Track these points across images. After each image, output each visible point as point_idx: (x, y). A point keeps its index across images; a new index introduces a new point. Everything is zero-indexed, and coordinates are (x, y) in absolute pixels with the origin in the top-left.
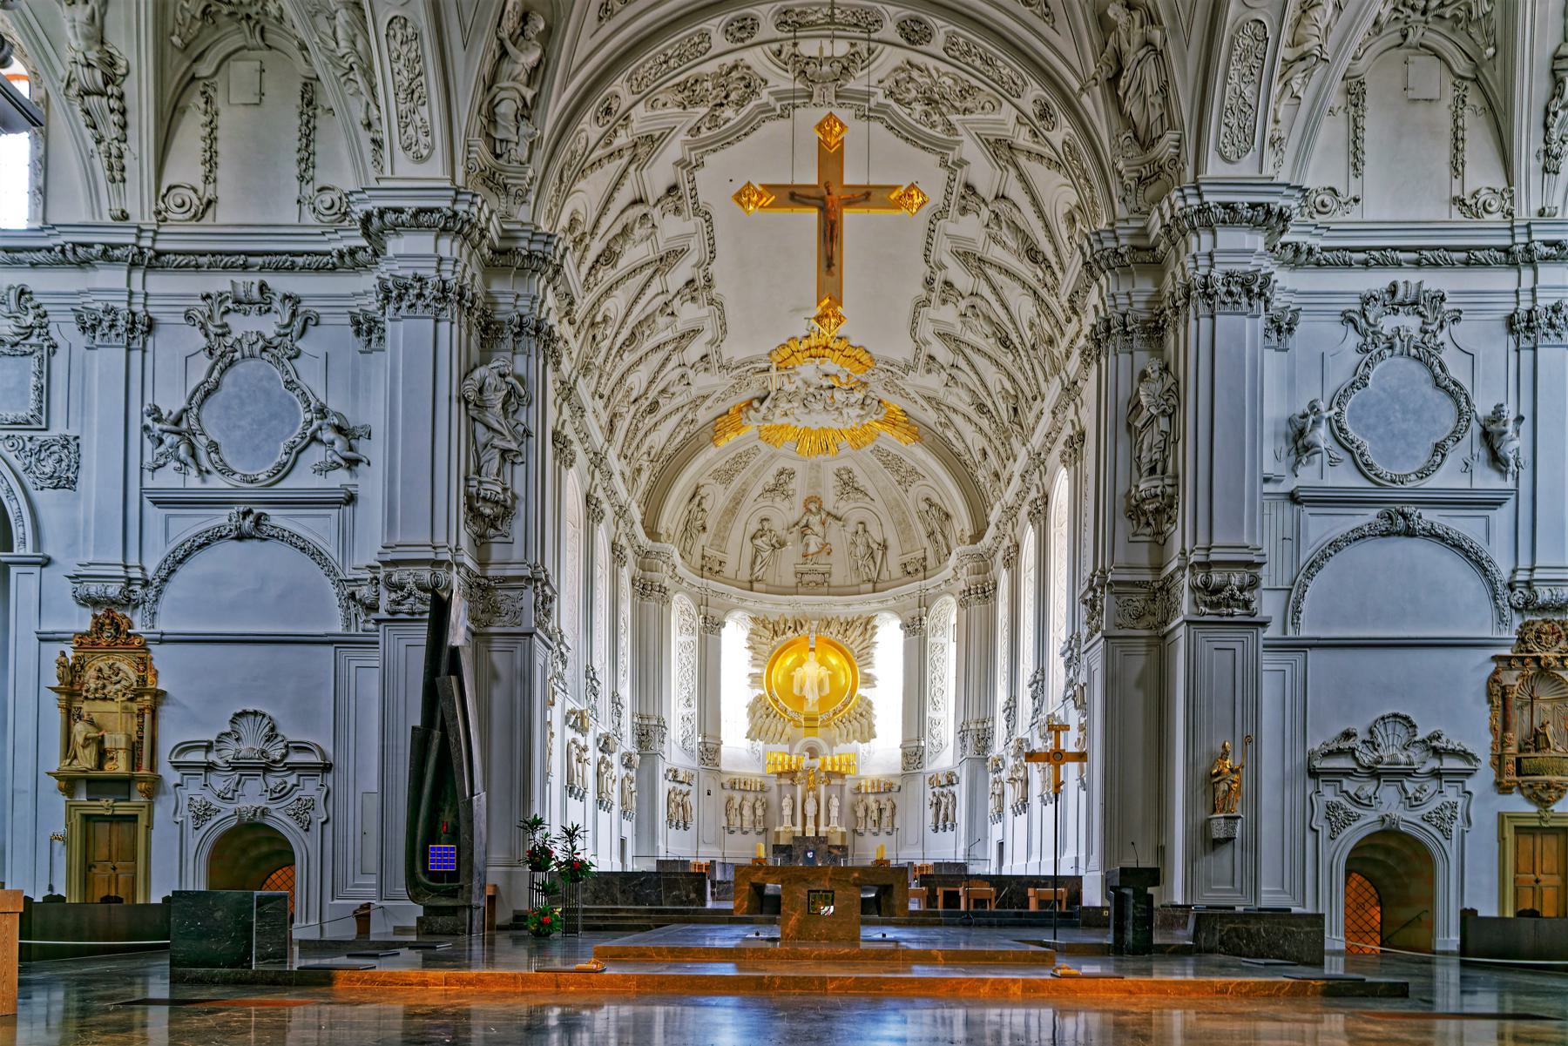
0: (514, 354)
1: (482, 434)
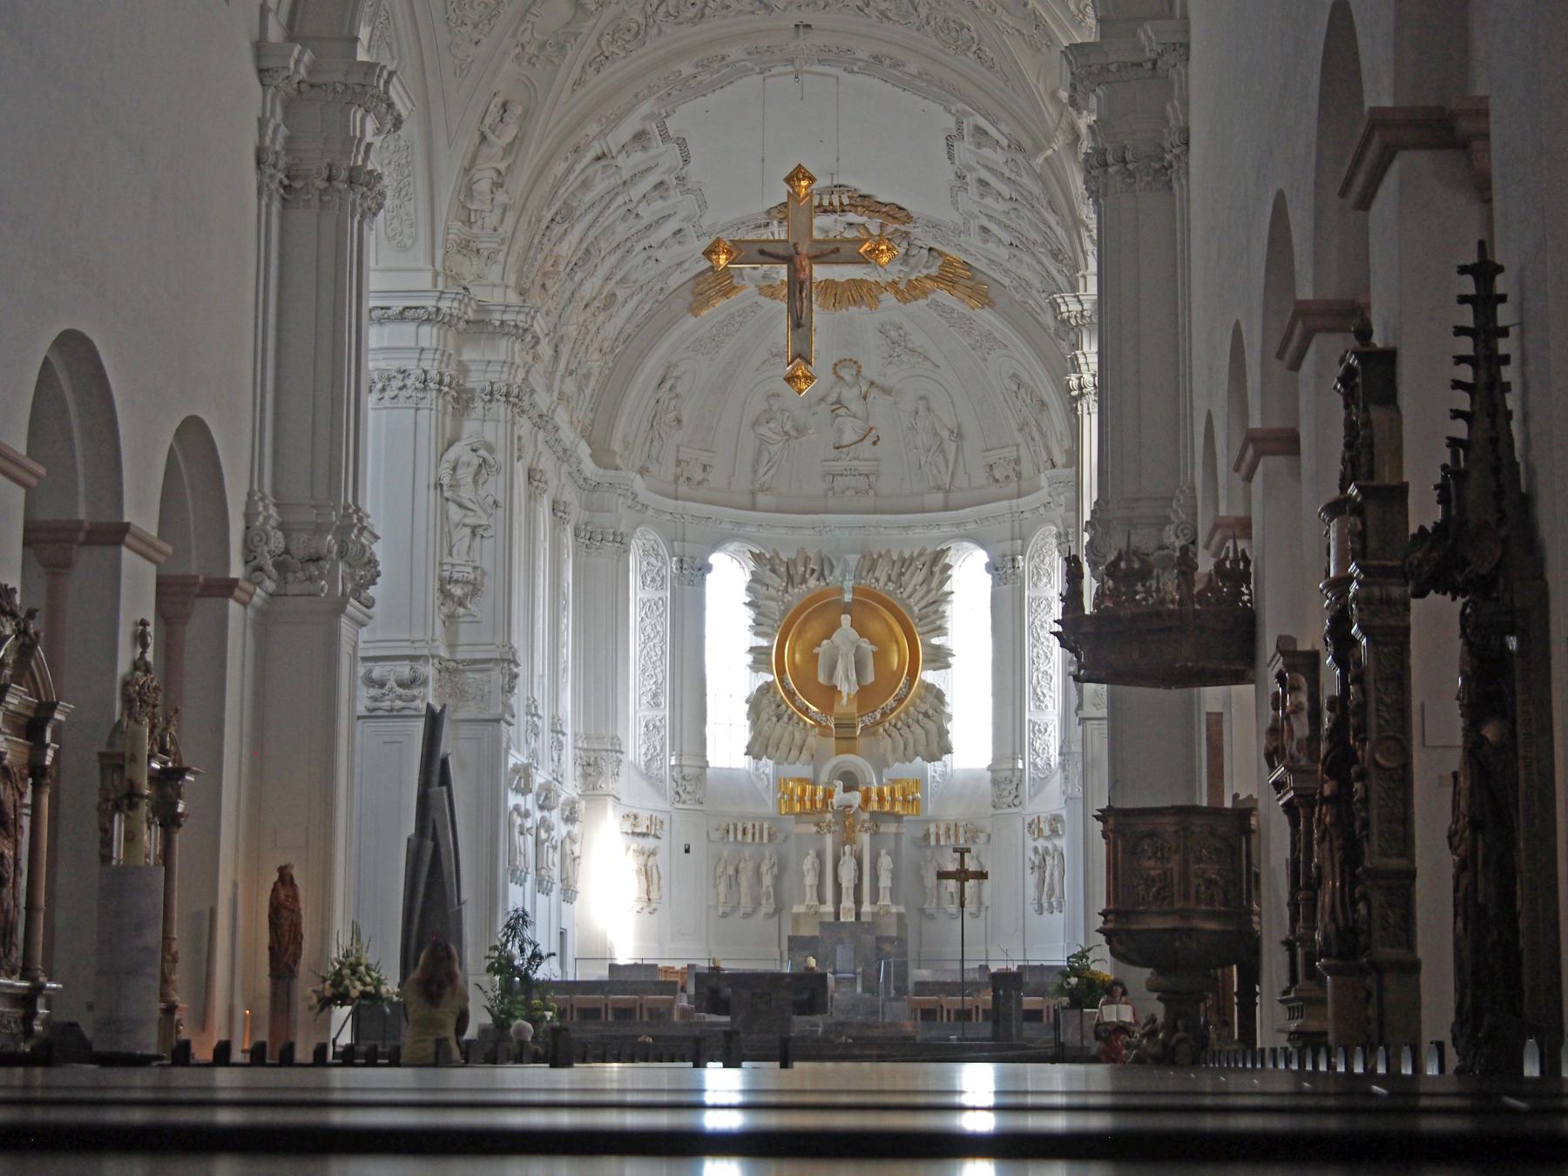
0: (484, 421)
1: (455, 513)
